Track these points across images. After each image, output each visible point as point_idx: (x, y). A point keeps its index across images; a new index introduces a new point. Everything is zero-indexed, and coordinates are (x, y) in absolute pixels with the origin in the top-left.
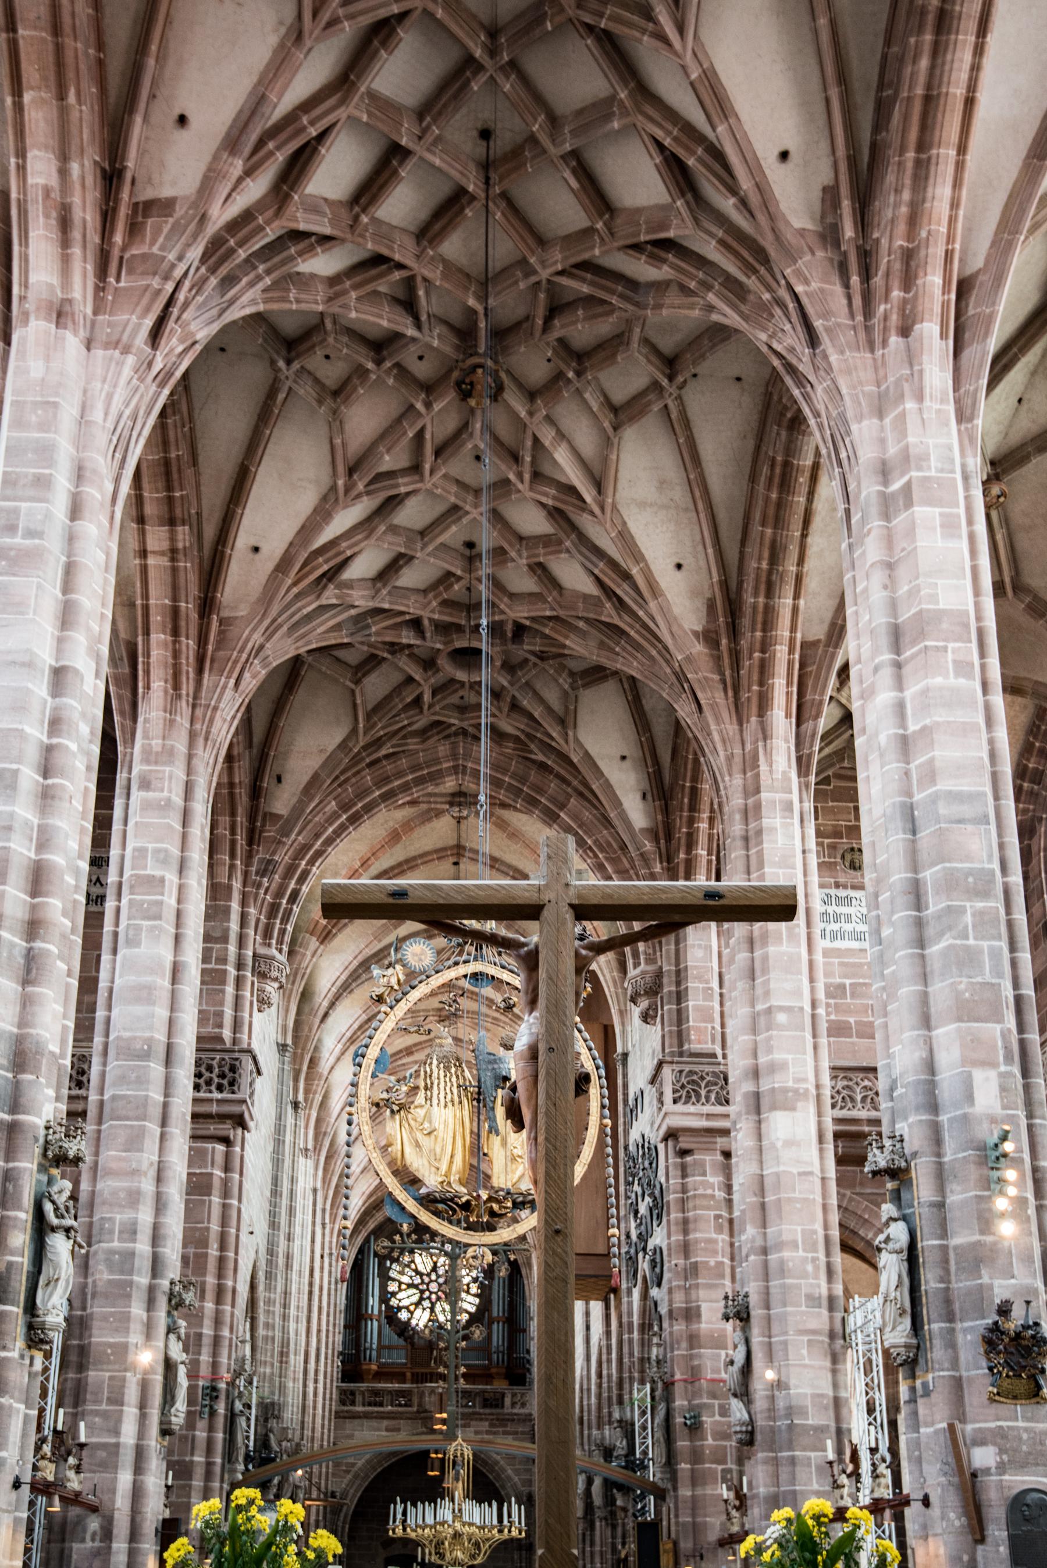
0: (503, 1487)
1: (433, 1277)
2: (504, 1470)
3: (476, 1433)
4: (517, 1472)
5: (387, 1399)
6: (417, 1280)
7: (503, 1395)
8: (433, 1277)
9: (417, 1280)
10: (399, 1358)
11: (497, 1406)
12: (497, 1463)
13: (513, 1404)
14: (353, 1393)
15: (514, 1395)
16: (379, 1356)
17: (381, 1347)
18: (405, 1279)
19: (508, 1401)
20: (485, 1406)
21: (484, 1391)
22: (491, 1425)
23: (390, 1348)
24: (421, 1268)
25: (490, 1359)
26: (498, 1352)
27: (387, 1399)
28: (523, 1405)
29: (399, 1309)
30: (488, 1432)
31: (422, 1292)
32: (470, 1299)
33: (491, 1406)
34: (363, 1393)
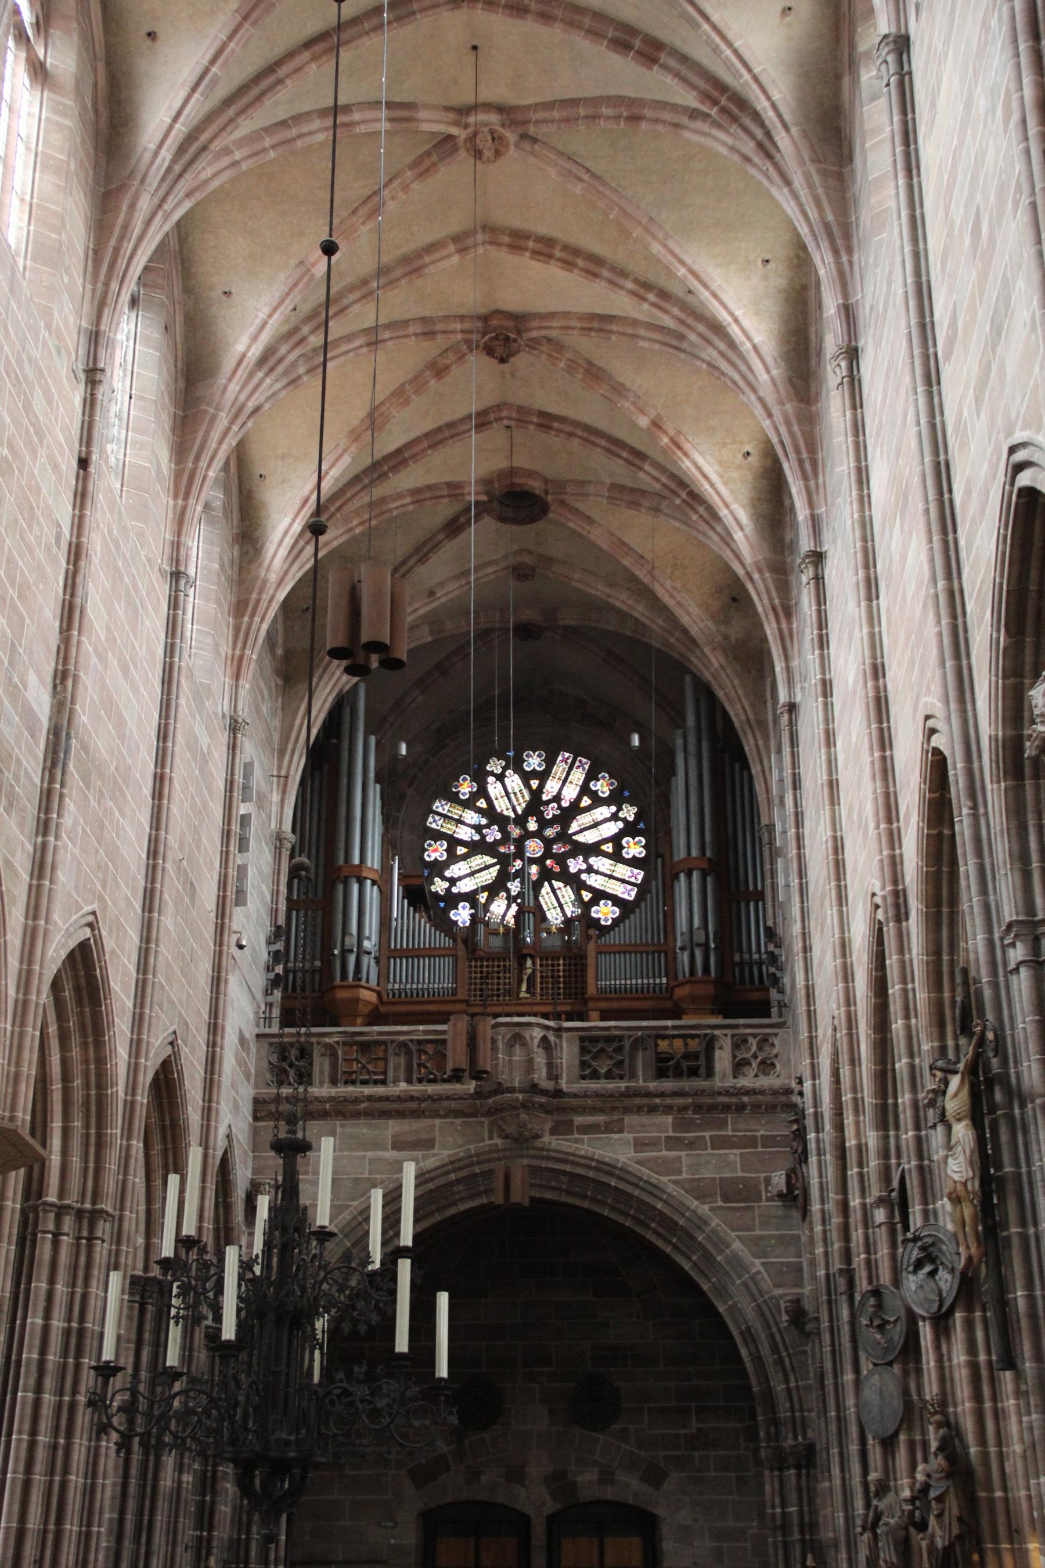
0: (722, 1291)
1: (532, 825)
2: (722, 1244)
3: (640, 1145)
4: (759, 1247)
5: (396, 1063)
6: (493, 834)
7: (710, 1044)
8: (532, 825)
9: (493, 834)
10: (435, 977)
11: (693, 1072)
12: (701, 1222)
13: (739, 1066)
14: (305, 1052)
15: (740, 1042)
16: (383, 976)
17: (387, 954)
18: (464, 833)
19: (723, 1059)
20: (661, 1074)
21: (659, 1035)
22: (680, 1125)
23: (413, 954)
24: (502, 806)
25: (671, 971)
26: (690, 946)
27: (396, 1063)
28: (767, 1066)
29: (452, 900)
30: (672, 1143)
31: (504, 861)
32: (623, 871)
33: (678, 1075)
34: (331, 1051)
